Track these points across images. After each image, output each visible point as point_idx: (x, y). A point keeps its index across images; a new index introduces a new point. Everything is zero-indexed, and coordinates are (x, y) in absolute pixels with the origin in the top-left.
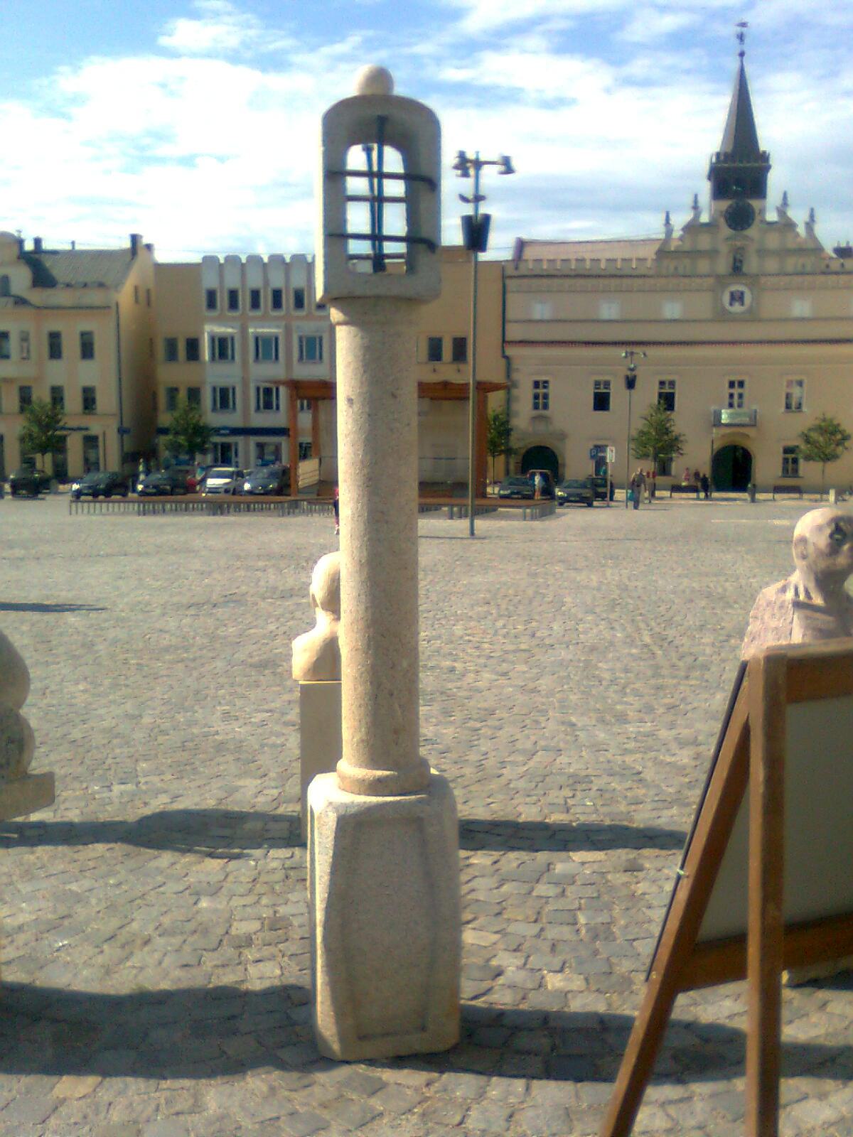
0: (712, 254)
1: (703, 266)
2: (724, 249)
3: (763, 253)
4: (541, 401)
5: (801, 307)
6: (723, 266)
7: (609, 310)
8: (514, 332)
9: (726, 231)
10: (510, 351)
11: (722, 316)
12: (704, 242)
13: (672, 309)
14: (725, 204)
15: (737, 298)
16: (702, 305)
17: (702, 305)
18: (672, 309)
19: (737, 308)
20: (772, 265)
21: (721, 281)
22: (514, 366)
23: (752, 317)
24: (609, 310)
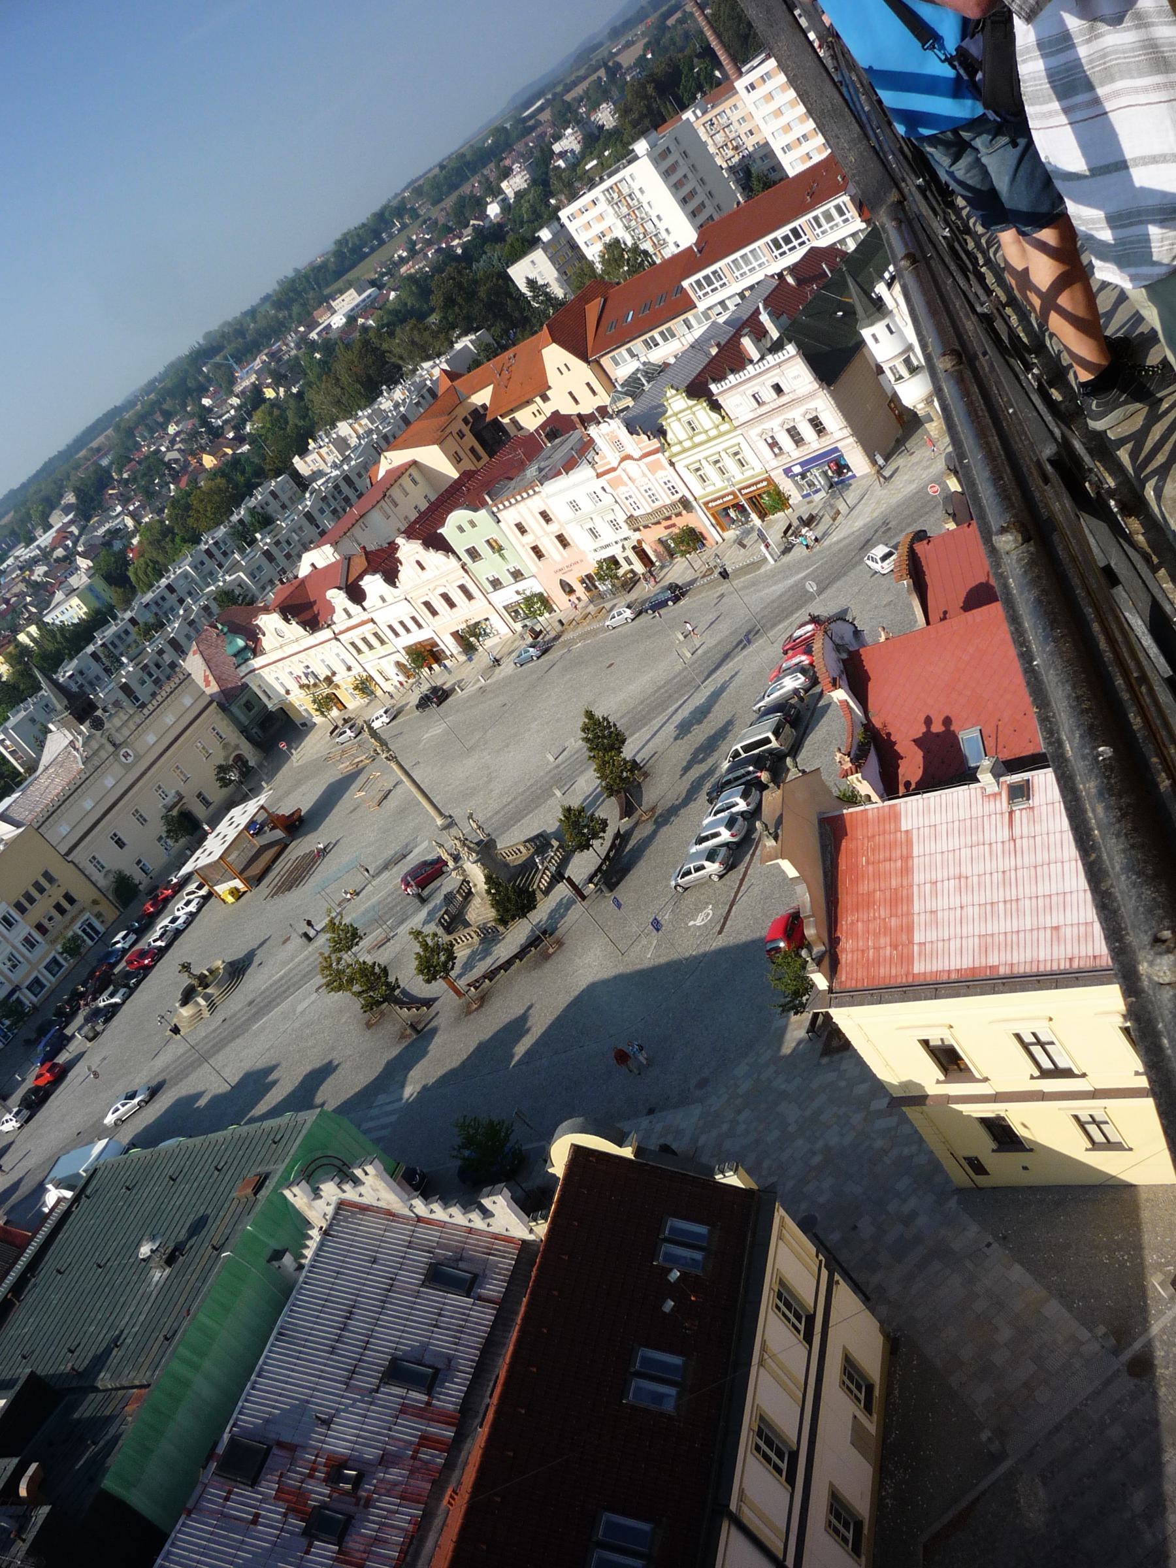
0: (101, 747)
1: (103, 754)
2: (104, 741)
3: (118, 730)
4: (100, 867)
5: (151, 738)
6: (111, 749)
7: (88, 804)
8: (63, 849)
9: (98, 733)
10: (69, 859)
11: (128, 768)
12: (95, 745)
13: (109, 781)
14: (87, 723)
15: (126, 755)
16: (117, 769)
17: (117, 769)
18: (109, 781)
19: (130, 759)
20: (126, 732)
21: (115, 754)
22: (76, 862)
23: (138, 757)
24: (88, 804)
